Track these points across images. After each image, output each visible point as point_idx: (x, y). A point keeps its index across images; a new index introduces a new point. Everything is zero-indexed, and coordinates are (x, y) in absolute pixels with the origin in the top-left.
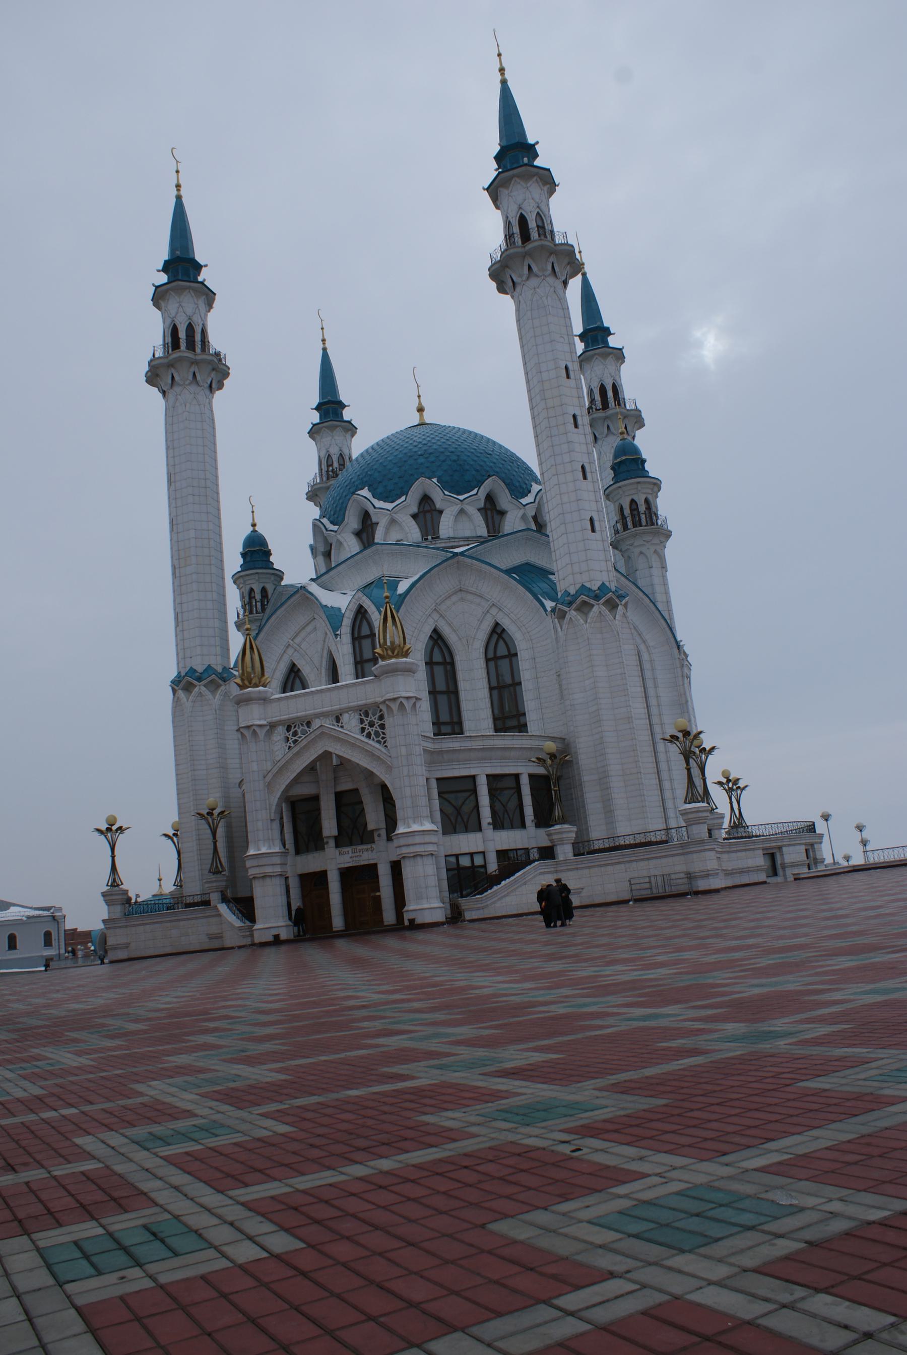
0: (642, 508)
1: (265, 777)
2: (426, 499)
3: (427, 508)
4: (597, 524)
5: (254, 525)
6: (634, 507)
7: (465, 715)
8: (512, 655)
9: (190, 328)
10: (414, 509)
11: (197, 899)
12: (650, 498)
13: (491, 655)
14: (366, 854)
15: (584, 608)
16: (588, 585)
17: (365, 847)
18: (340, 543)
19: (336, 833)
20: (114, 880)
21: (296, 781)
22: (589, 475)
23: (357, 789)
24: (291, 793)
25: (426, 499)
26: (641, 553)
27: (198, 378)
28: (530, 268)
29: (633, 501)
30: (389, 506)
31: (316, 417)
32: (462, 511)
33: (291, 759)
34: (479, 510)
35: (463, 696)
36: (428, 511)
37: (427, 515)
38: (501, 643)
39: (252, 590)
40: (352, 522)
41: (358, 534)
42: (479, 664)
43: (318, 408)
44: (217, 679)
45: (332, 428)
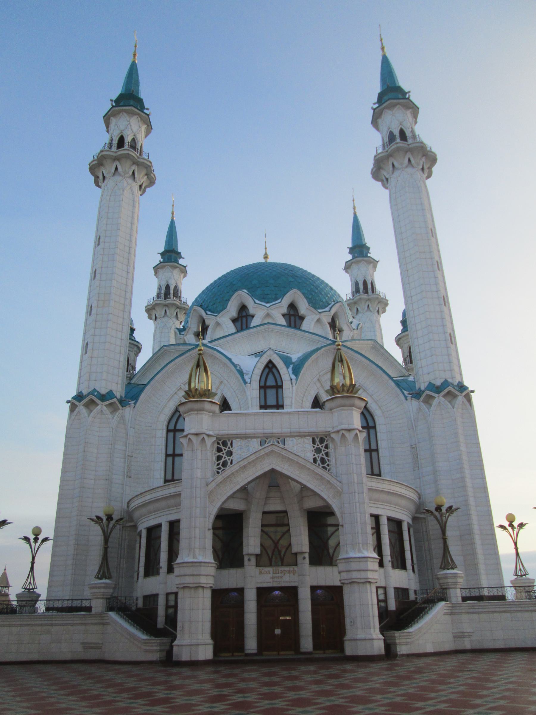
1: (207, 485)
2: (292, 306)
3: (292, 312)
11: (66, 604)
14: (287, 575)
16: (450, 380)
17: (287, 569)
18: (218, 324)
19: (258, 551)
21: (232, 496)
22: (447, 304)
23: (286, 512)
24: (225, 506)
25: (292, 306)
30: (268, 305)
31: (159, 258)
32: (319, 321)
33: (237, 471)
36: (292, 315)
40: (232, 310)
41: (234, 321)
43: (163, 254)
44: (117, 403)
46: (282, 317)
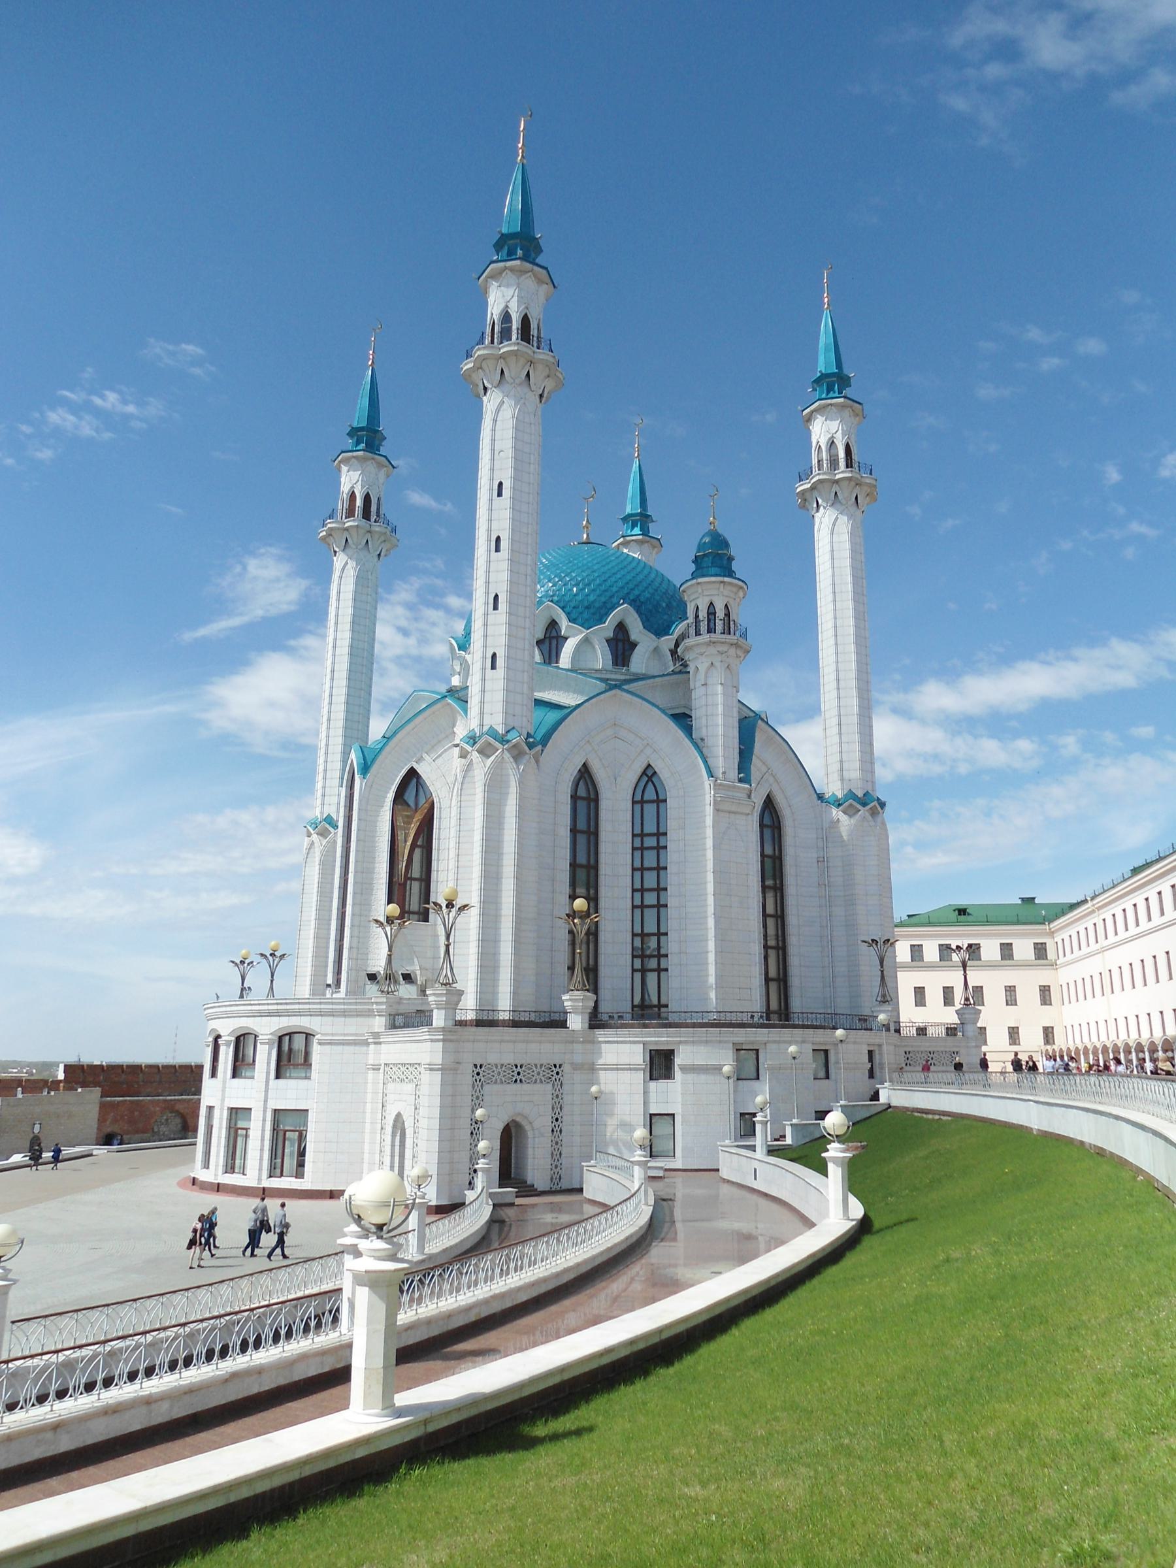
7: (603, 858)
35: (603, 836)
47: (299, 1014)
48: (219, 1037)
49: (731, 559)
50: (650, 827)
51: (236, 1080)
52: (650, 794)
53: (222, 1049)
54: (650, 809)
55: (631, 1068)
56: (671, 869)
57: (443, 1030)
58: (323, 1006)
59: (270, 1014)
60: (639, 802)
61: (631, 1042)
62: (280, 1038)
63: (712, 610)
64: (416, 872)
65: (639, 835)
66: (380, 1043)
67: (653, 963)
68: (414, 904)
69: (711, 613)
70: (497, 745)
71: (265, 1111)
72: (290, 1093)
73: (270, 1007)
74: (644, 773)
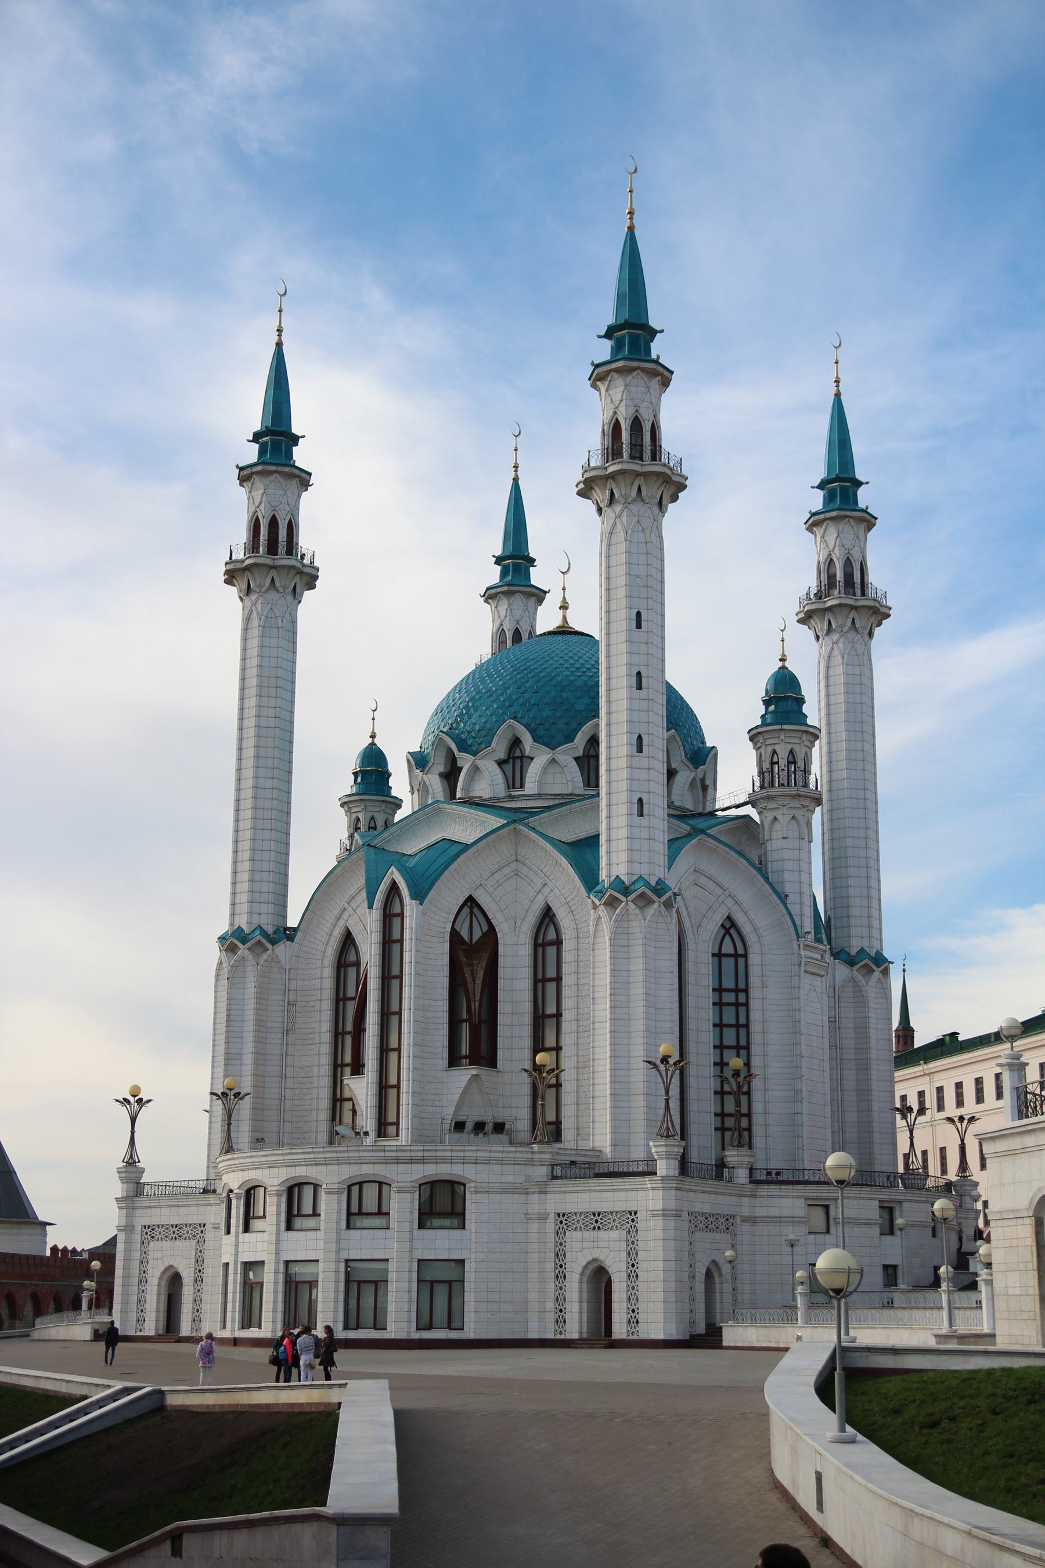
0: (783, 763)
3: (518, 753)
4: (645, 807)
5: (373, 736)
6: (775, 759)
8: (558, 943)
9: (273, 523)
10: (502, 755)
12: (796, 748)
13: (540, 941)
15: (612, 903)
20: (131, 1157)
26: (775, 818)
27: (278, 584)
28: (612, 494)
29: (775, 752)
32: (554, 761)
34: (576, 759)
36: (518, 757)
37: (514, 762)
38: (552, 928)
39: (358, 819)
42: (525, 951)
45: (508, 594)
46: (496, 766)
47: (451, 1161)
48: (231, 1191)
49: (801, 701)
50: (728, 983)
51: (352, 1232)
52: (728, 948)
53: (234, 1203)
54: (728, 964)
55: (794, 1221)
56: (755, 1027)
57: (664, 1179)
58: (479, 1154)
59: (411, 1161)
60: (719, 955)
61: (793, 1197)
62: (420, 1185)
63: (791, 759)
64: (484, 1016)
65: (719, 990)
66: (546, 1193)
67: (729, 1122)
68: (484, 1049)
69: (792, 760)
70: (654, 897)
71: (411, 1261)
72: (441, 1243)
73: (413, 1154)
74: (722, 925)
